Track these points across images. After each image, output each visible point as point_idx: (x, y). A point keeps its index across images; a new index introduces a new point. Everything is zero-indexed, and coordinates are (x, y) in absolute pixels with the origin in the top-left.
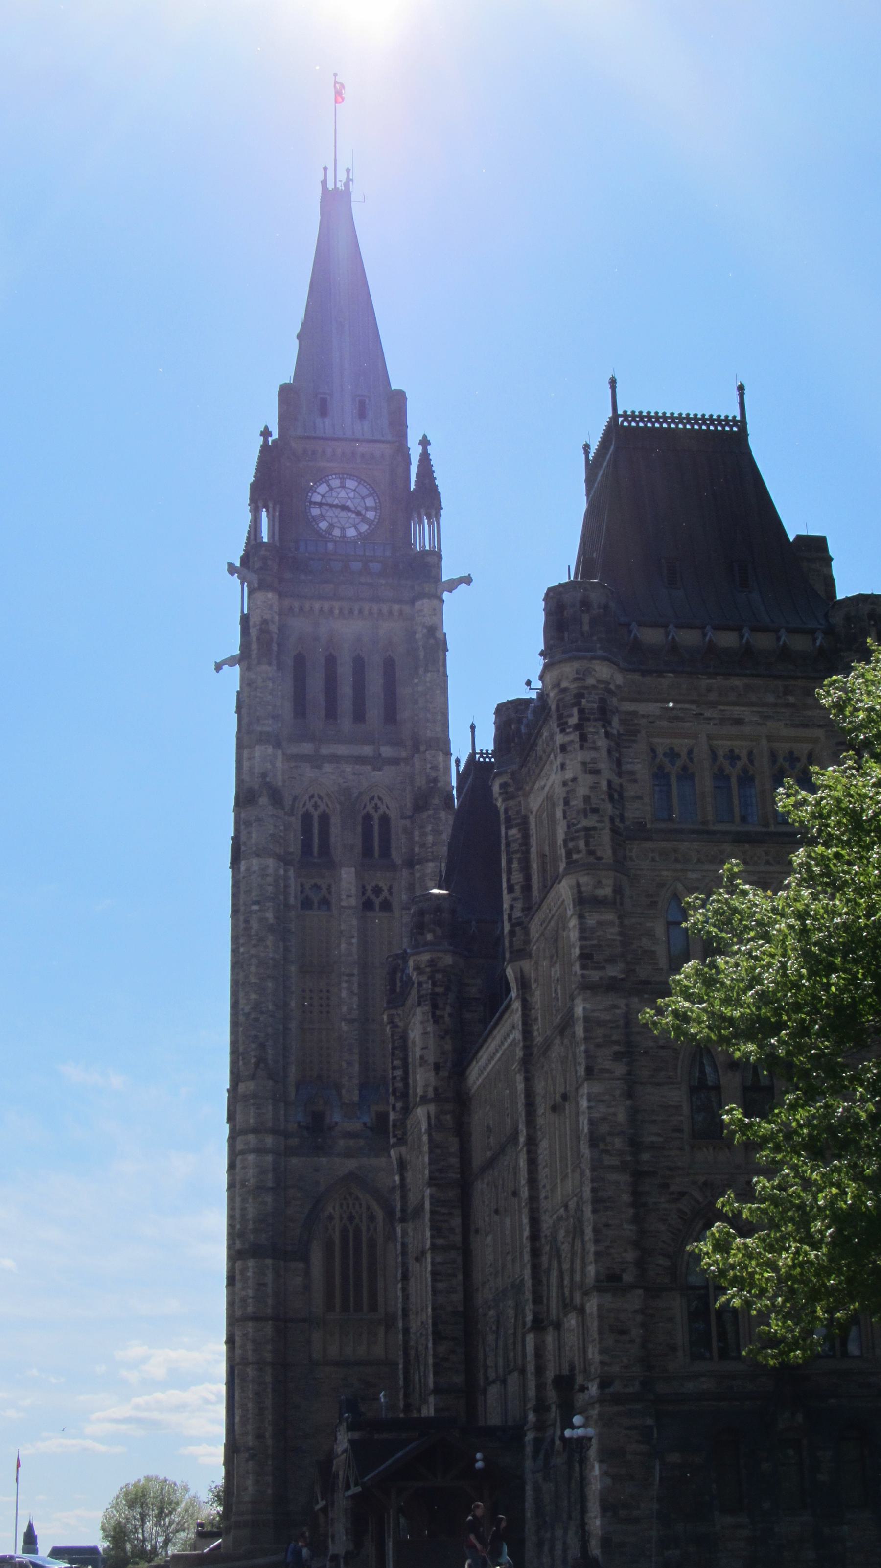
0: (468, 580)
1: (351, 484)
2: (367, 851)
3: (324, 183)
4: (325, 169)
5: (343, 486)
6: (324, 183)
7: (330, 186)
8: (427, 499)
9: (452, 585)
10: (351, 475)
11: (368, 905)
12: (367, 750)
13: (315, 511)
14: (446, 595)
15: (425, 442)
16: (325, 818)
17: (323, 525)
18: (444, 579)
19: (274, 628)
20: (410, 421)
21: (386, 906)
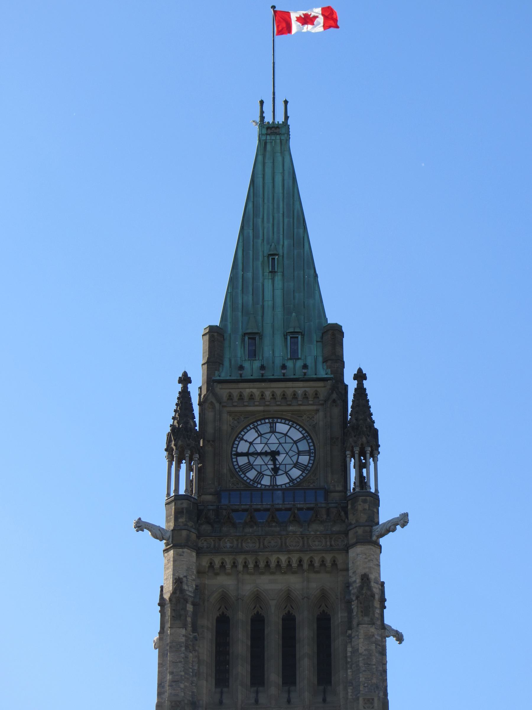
0: (403, 520)
1: (282, 427)
3: (262, 118)
4: (262, 102)
5: (273, 431)
6: (262, 118)
7: (268, 119)
9: (391, 527)
10: (282, 419)
13: (242, 461)
14: (382, 541)
15: (360, 376)
17: (252, 474)
18: (381, 522)
19: (189, 588)
20: (346, 358)
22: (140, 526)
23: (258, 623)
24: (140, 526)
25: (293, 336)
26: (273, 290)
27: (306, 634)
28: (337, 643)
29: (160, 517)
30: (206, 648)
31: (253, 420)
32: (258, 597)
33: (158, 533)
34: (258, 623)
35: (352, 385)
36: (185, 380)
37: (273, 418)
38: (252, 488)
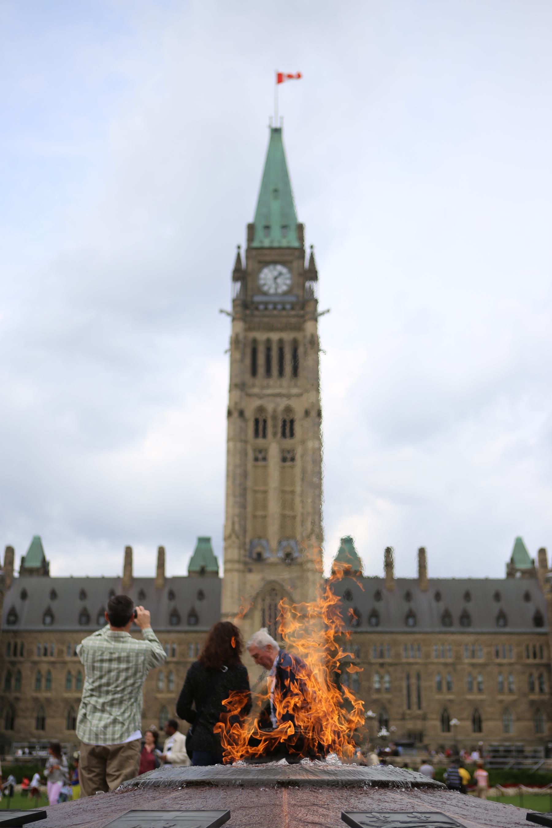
2: (284, 435)
8: (312, 274)
9: (323, 314)
11: (284, 460)
12: (284, 391)
15: (312, 247)
16: (265, 421)
19: (241, 337)
21: (293, 459)
22: (222, 311)
23: (269, 349)
24: (222, 311)
25: (284, 227)
26: (275, 206)
27: (288, 357)
28: (301, 360)
29: (229, 307)
30: (248, 361)
31: (266, 264)
32: (269, 341)
33: (228, 314)
34: (269, 349)
35: (308, 252)
36: (239, 247)
37: (275, 262)
38: (265, 294)
